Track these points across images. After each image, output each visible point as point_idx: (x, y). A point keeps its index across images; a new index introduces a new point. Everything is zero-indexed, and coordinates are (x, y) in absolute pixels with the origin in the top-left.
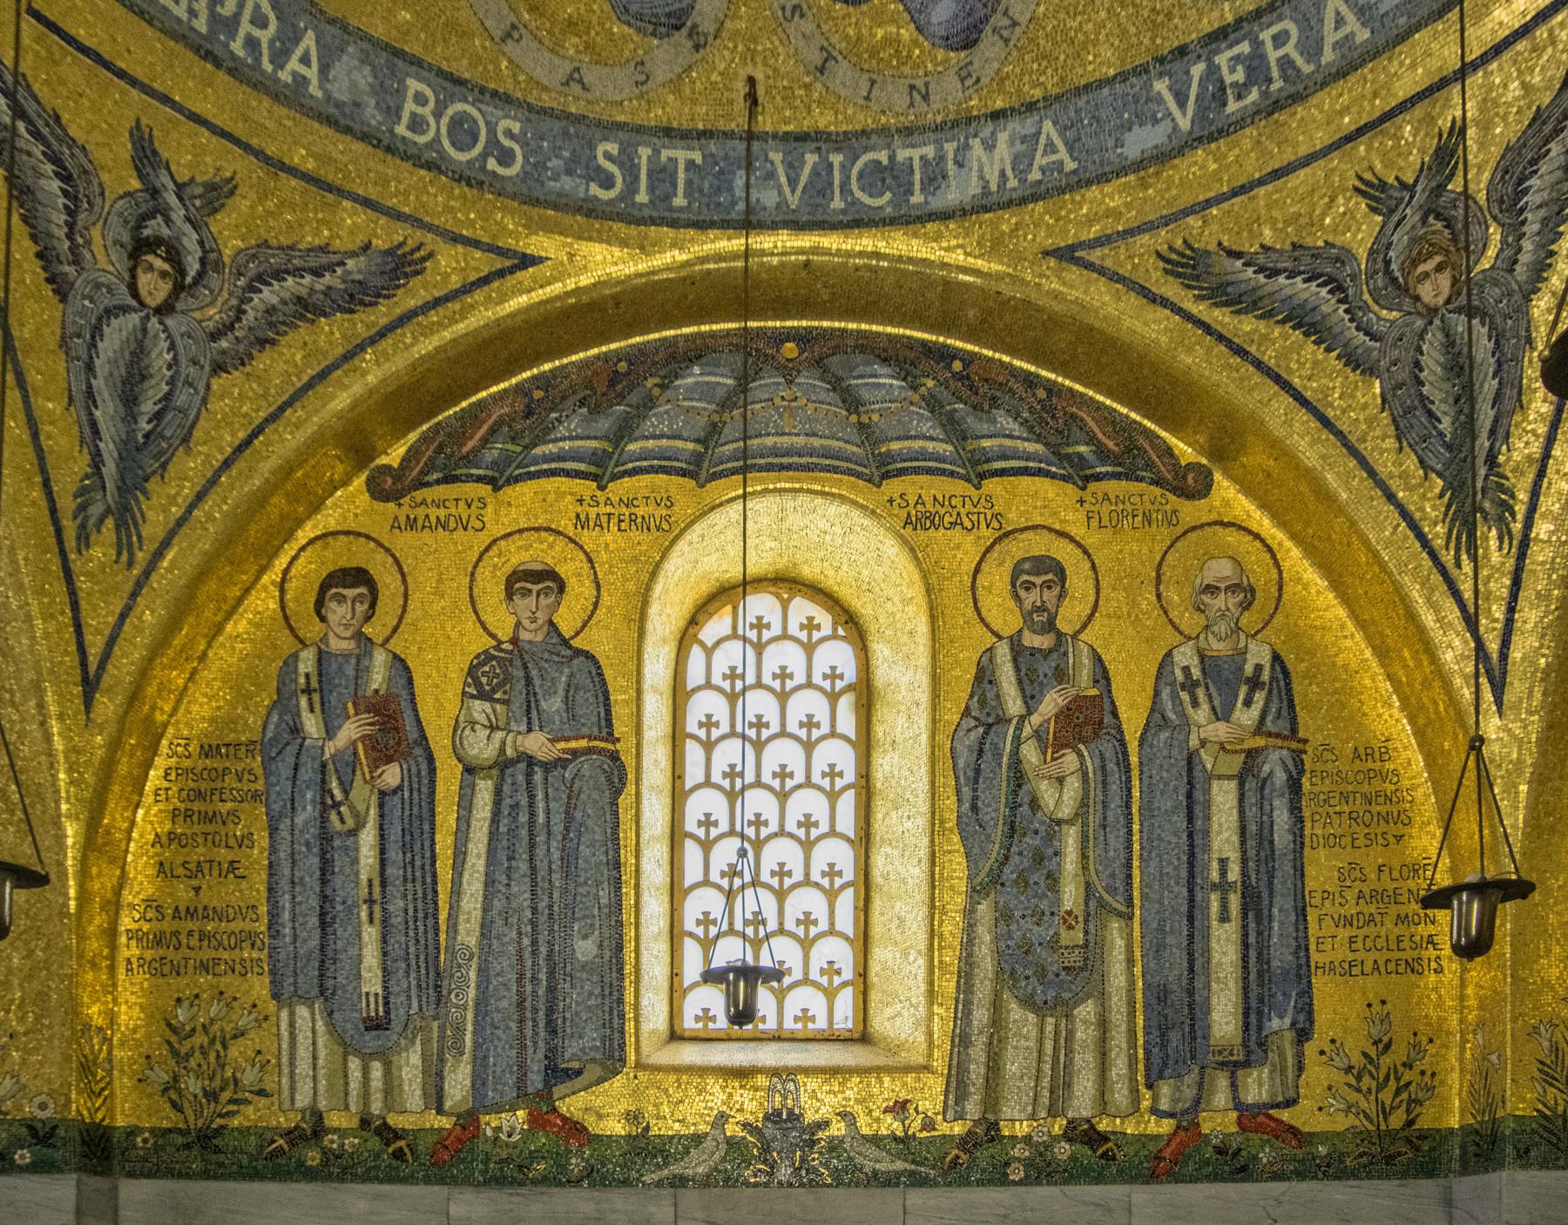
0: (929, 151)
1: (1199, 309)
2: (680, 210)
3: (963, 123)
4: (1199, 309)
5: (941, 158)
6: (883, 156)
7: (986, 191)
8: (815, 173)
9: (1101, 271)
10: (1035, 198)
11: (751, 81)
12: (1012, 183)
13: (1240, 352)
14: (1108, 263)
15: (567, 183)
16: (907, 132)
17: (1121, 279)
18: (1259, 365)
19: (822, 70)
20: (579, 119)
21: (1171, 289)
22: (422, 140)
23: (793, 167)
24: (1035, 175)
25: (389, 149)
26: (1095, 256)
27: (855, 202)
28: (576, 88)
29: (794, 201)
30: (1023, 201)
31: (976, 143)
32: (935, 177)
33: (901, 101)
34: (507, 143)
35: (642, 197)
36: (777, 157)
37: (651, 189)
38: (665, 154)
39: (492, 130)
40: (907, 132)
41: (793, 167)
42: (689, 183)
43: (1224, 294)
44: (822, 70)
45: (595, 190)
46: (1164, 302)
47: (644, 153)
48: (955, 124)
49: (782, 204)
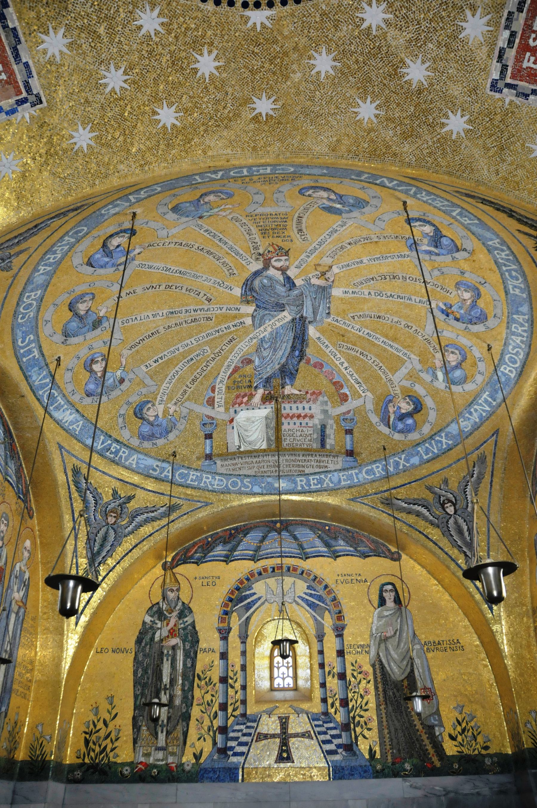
0: (63, 403)
1: (71, 483)
2: (22, 361)
3: (72, 405)
4: (71, 483)
5: (63, 406)
6: (56, 394)
7: (61, 421)
8: (45, 383)
9: (62, 457)
10: (67, 431)
11: (59, 357)
12: (66, 424)
13: (71, 499)
14: (65, 457)
15: (20, 334)
16: (64, 396)
17: (64, 463)
18: (72, 504)
19: (68, 370)
20: (37, 327)
21: (70, 474)
22: (25, 300)
23: (44, 378)
24: (71, 428)
25: (21, 294)
26: (64, 453)
27: (43, 396)
28: (45, 323)
29: (37, 383)
30: (64, 429)
31: (70, 411)
32: (57, 408)
33: (70, 390)
34: (27, 317)
35: (22, 351)
36: (45, 373)
37: (25, 352)
38: (35, 350)
39: (29, 312)
40: (64, 396)
41: (44, 378)
42: (30, 359)
43: (77, 484)
44: (68, 370)
45: (20, 341)
46: (66, 475)
47: (33, 345)
48: (71, 404)
49: (34, 381)
